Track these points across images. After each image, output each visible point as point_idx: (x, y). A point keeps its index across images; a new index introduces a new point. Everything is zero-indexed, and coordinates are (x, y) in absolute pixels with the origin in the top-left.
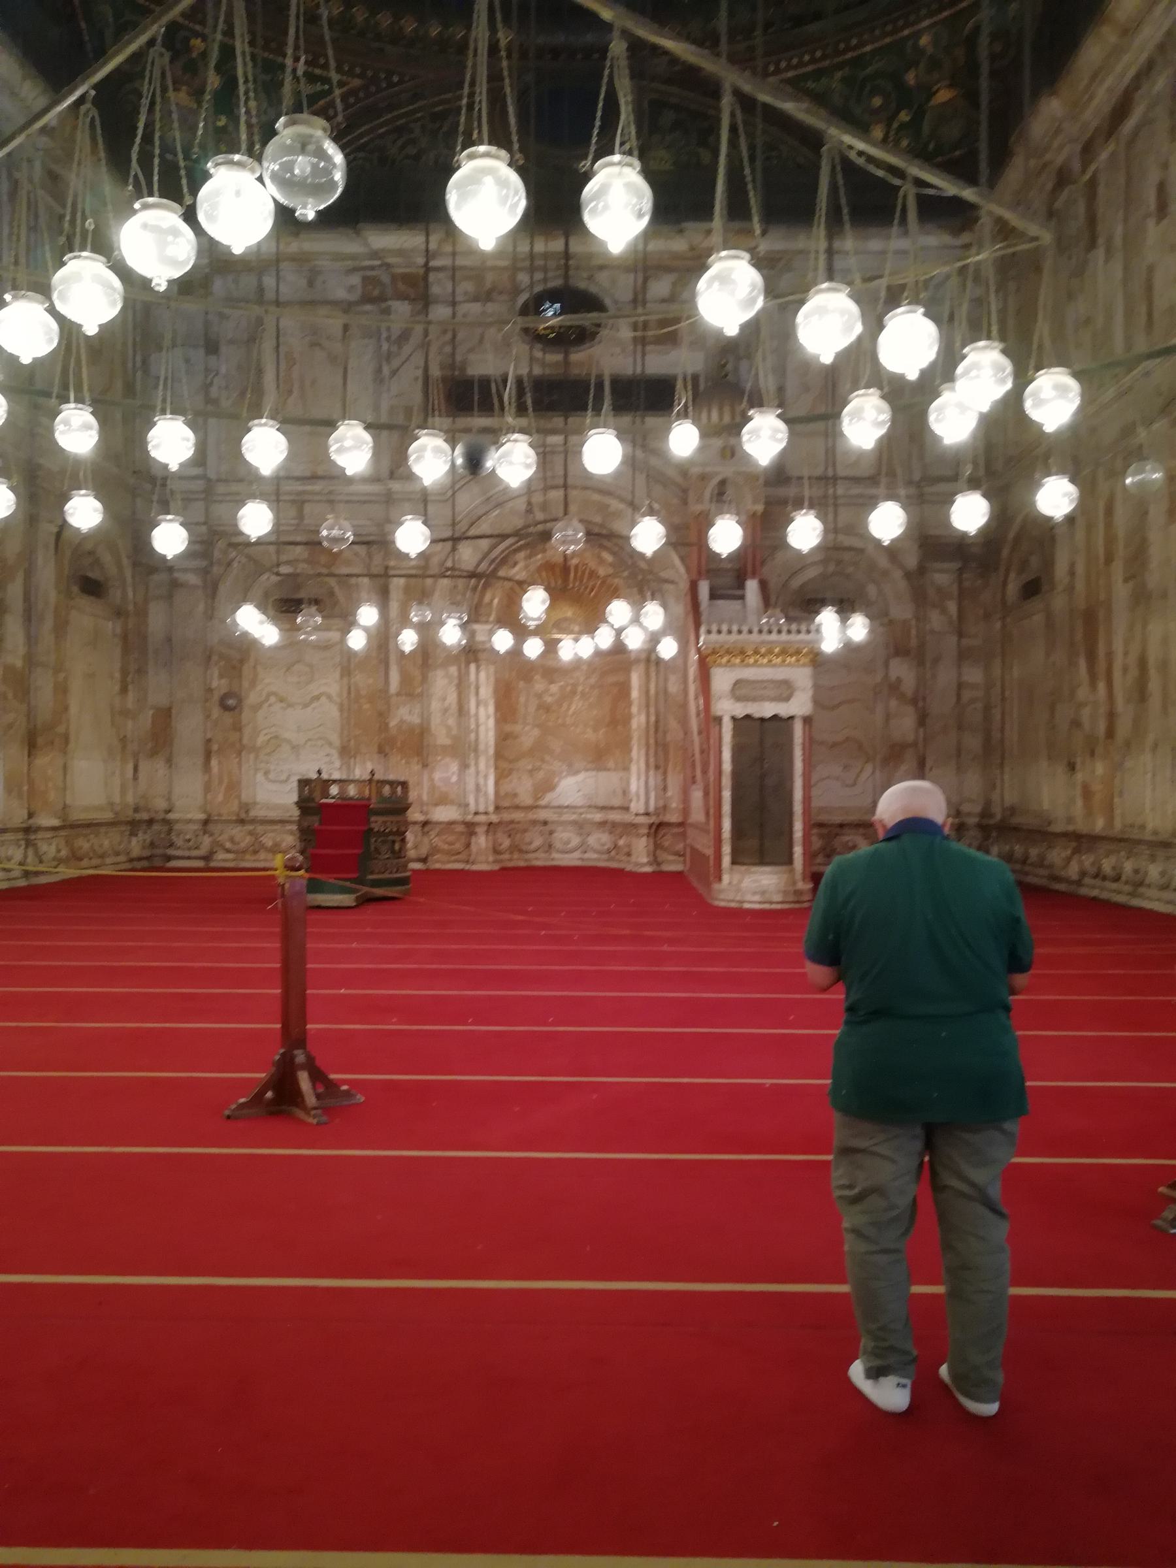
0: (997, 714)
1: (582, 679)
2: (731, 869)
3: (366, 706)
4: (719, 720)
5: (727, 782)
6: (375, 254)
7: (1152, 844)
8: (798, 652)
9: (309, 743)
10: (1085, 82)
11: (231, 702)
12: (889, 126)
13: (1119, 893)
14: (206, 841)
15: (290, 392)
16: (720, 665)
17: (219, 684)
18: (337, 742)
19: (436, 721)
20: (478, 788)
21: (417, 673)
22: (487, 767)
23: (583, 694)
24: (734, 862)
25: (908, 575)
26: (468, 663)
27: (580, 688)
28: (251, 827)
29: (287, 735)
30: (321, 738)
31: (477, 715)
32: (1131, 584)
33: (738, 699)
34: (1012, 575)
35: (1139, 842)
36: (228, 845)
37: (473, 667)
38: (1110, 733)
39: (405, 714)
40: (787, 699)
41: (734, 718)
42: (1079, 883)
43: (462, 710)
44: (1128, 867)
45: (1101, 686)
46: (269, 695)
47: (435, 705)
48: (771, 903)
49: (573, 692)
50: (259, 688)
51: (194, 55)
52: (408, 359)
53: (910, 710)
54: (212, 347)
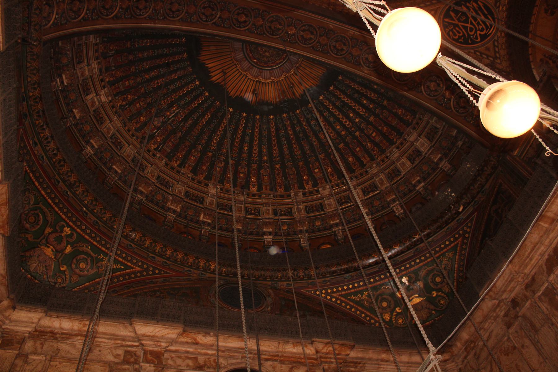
6: (138, 338)
10: (529, 251)
12: (392, 314)
51: (63, 235)
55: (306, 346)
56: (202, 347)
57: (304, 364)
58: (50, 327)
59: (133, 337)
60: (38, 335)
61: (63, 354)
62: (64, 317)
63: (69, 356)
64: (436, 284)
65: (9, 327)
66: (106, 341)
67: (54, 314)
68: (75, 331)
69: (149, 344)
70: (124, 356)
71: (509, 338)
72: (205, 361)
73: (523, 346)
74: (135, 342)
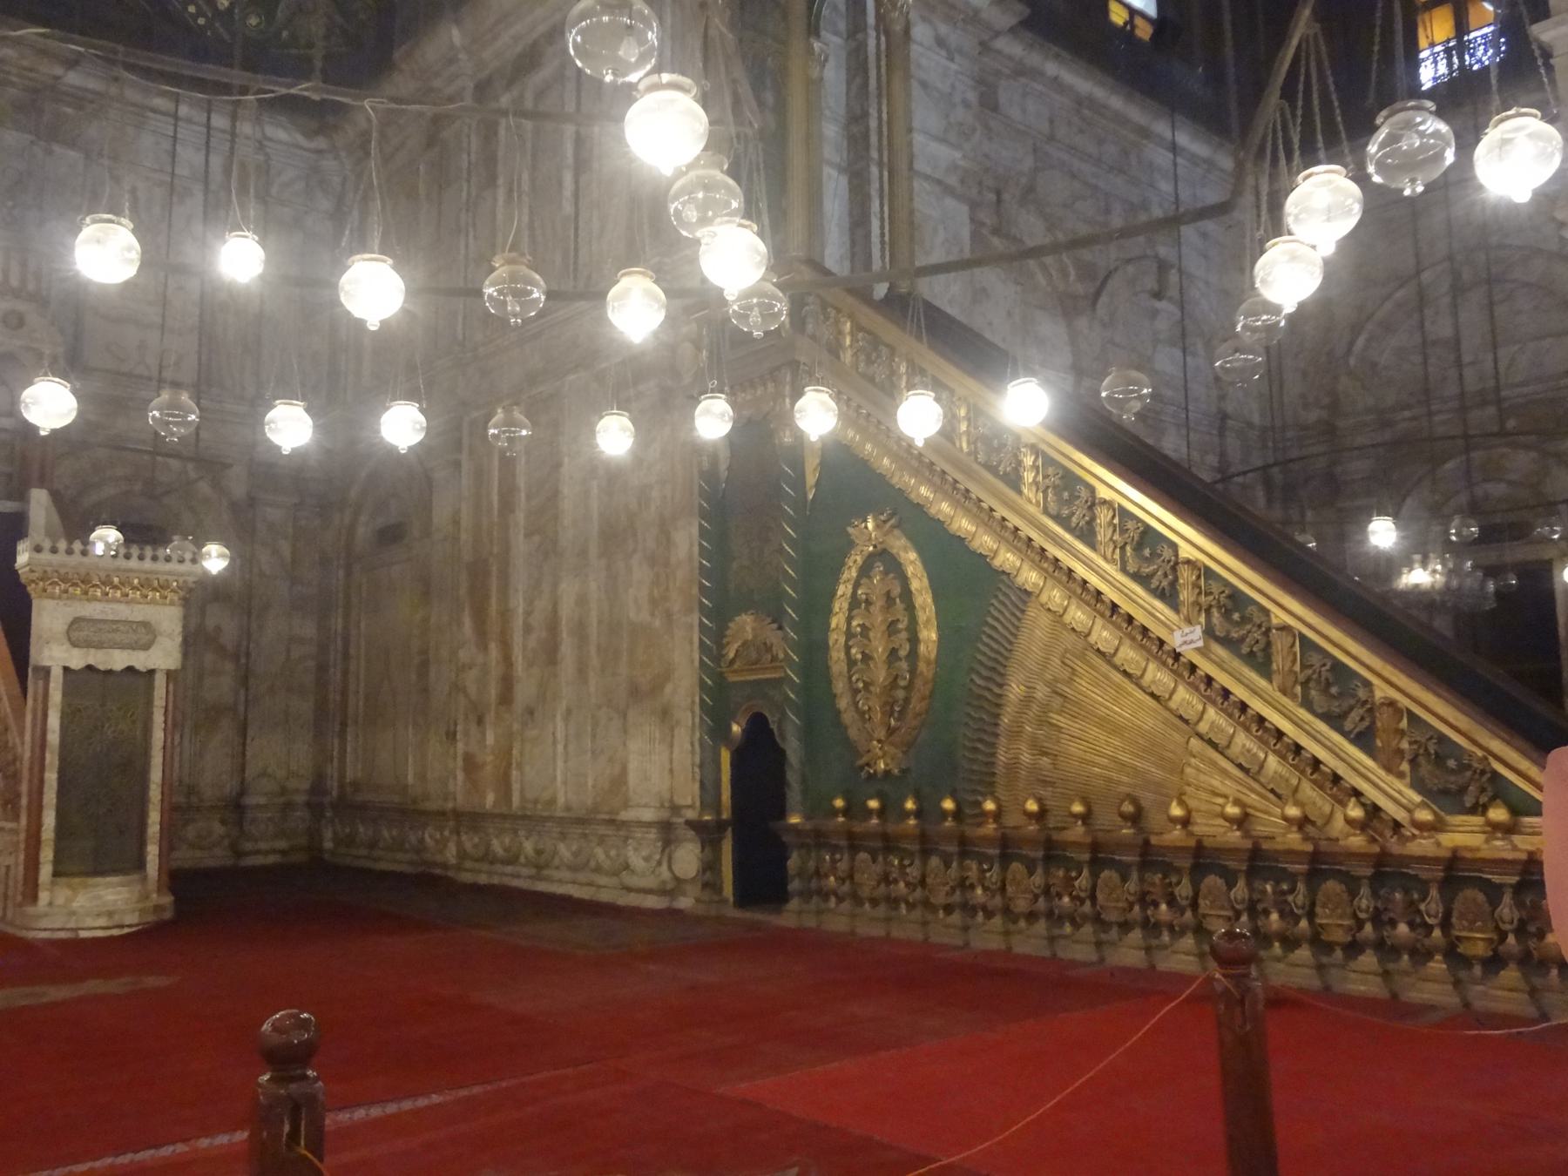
0: (335, 675)
2: (53, 883)
4: (46, 672)
5: (52, 759)
7: (561, 821)
8: (164, 586)
13: (518, 876)
16: (52, 597)
24: (56, 874)
25: (234, 507)
32: (536, 538)
33: (75, 645)
34: (363, 518)
35: (550, 818)
38: (506, 698)
40: (146, 647)
41: (66, 669)
42: (459, 868)
44: (528, 846)
45: (494, 648)
48: (121, 926)
53: (229, 666)
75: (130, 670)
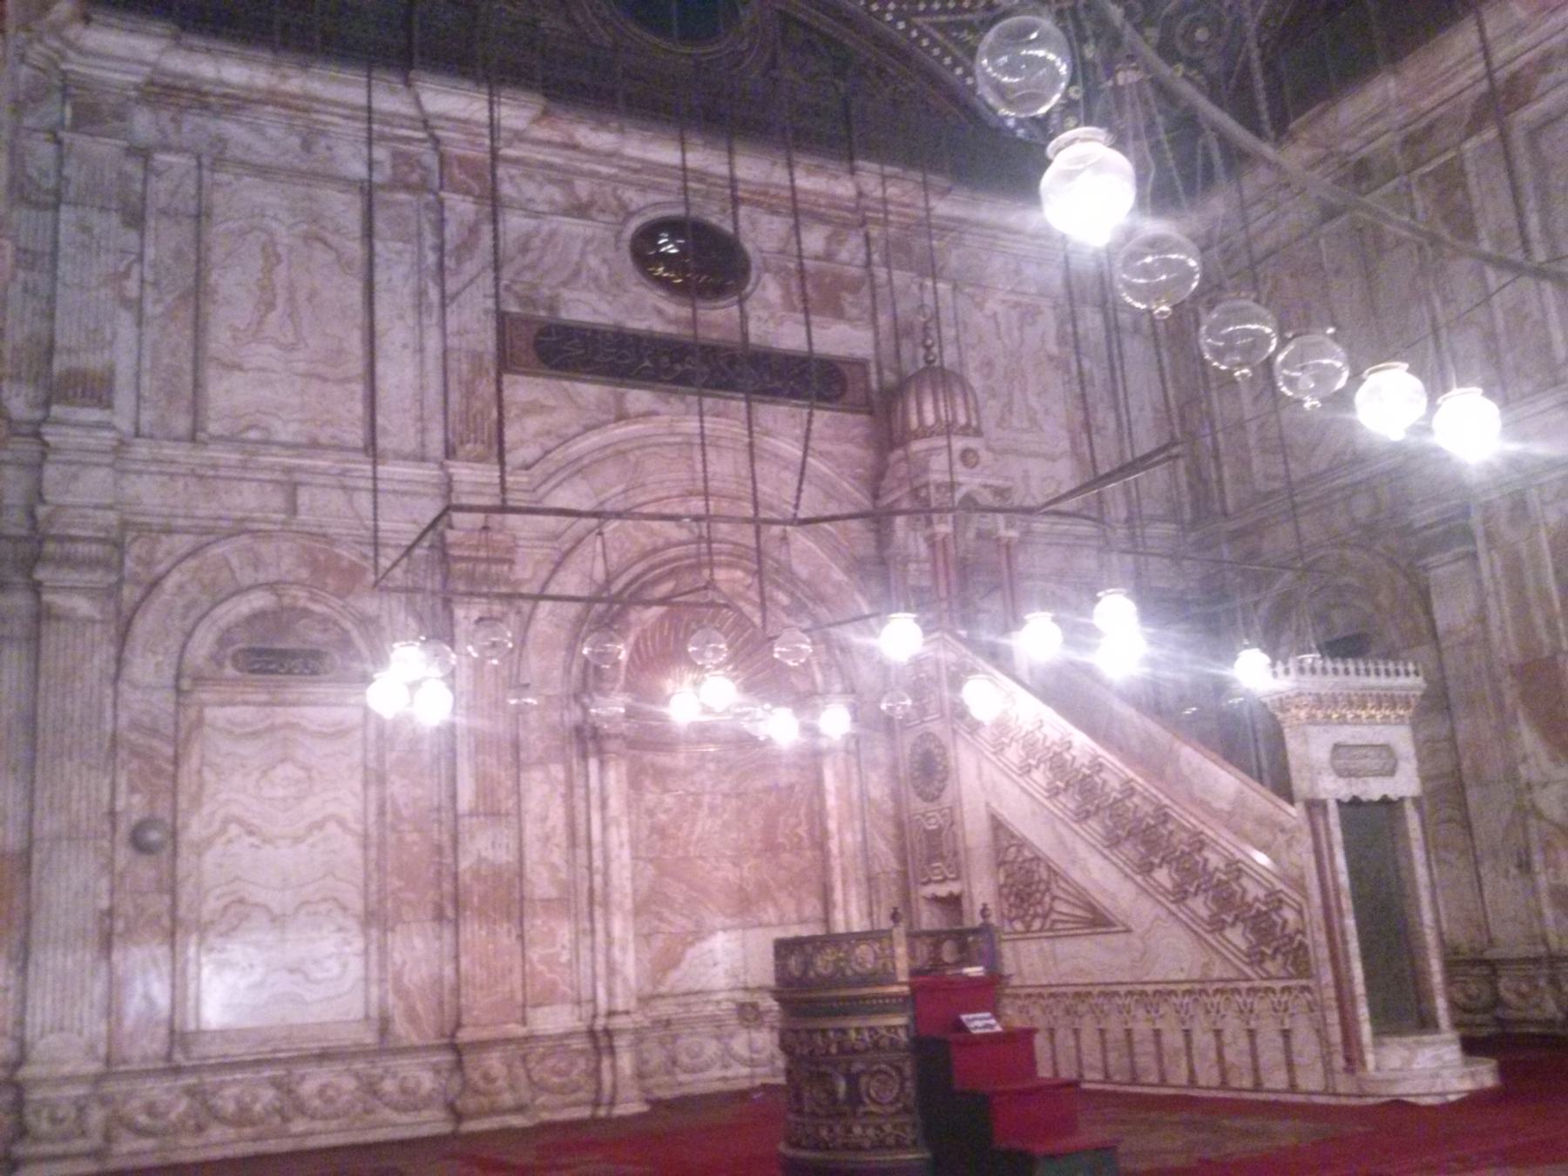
1: (709, 783)
3: (412, 837)
5: (1347, 904)
9: (303, 911)
11: (154, 836)
14: (96, 1116)
15: (271, 306)
17: (133, 806)
18: (357, 905)
19: (532, 855)
20: (612, 970)
21: (504, 777)
22: (625, 929)
23: (712, 808)
24: (1378, 1033)
26: (584, 756)
27: (707, 799)
28: (191, 1080)
29: (262, 896)
30: (325, 900)
31: (604, 844)
36: (143, 1119)
37: (593, 764)
39: (484, 847)
40: (1392, 772)
41: (1339, 802)
43: (576, 837)
46: (226, 822)
47: (531, 830)
49: (697, 805)
50: (206, 810)
52: (472, 281)
54: (135, 218)
55: (837, 177)
56: (584, 157)
57: (821, 219)
58: (188, 77)
59: (412, 119)
60: (156, 95)
61: (238, 153)
62: (227, 53)
63: (254, 158)
64: (1194, 46)
65: (77, 68)
66: (342, 122)
67: (196, 41)
68: (259, 91)
69: (453, 140)
70: (394, 167)
71: (1316, 243)
72: (592, 194)
73: (1338, 272)
74: (416, 130)
75: (1385, 801)
